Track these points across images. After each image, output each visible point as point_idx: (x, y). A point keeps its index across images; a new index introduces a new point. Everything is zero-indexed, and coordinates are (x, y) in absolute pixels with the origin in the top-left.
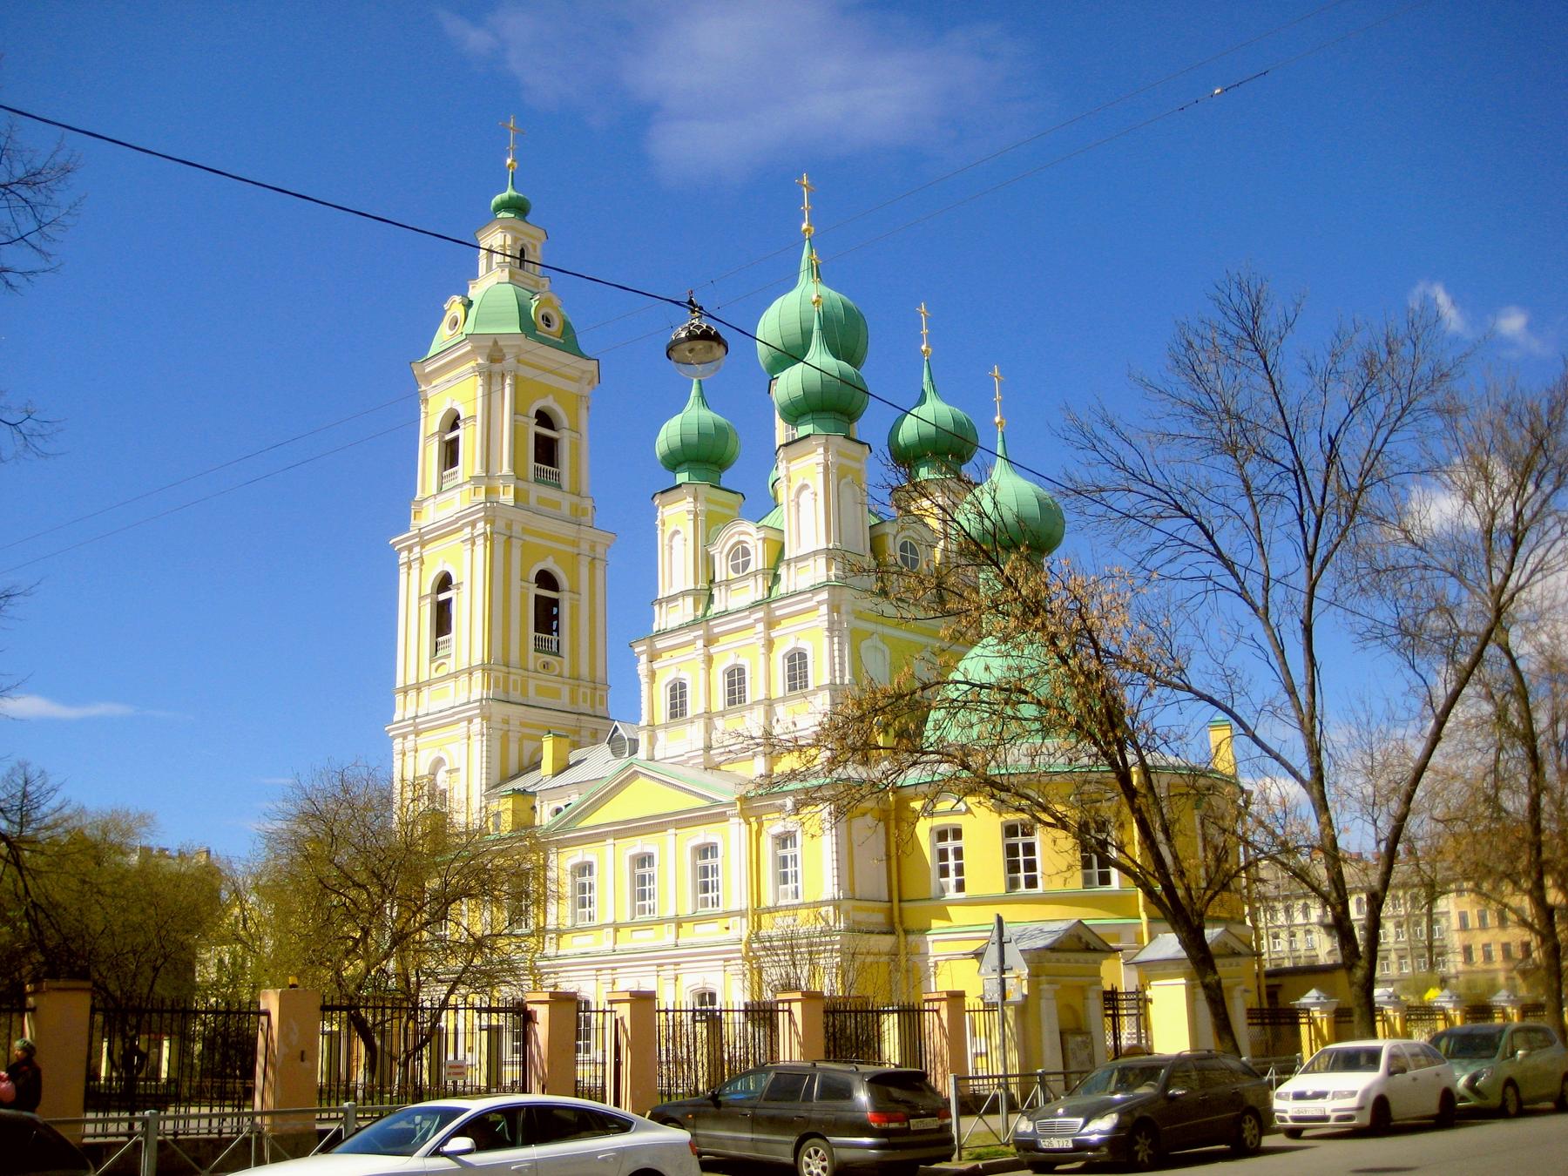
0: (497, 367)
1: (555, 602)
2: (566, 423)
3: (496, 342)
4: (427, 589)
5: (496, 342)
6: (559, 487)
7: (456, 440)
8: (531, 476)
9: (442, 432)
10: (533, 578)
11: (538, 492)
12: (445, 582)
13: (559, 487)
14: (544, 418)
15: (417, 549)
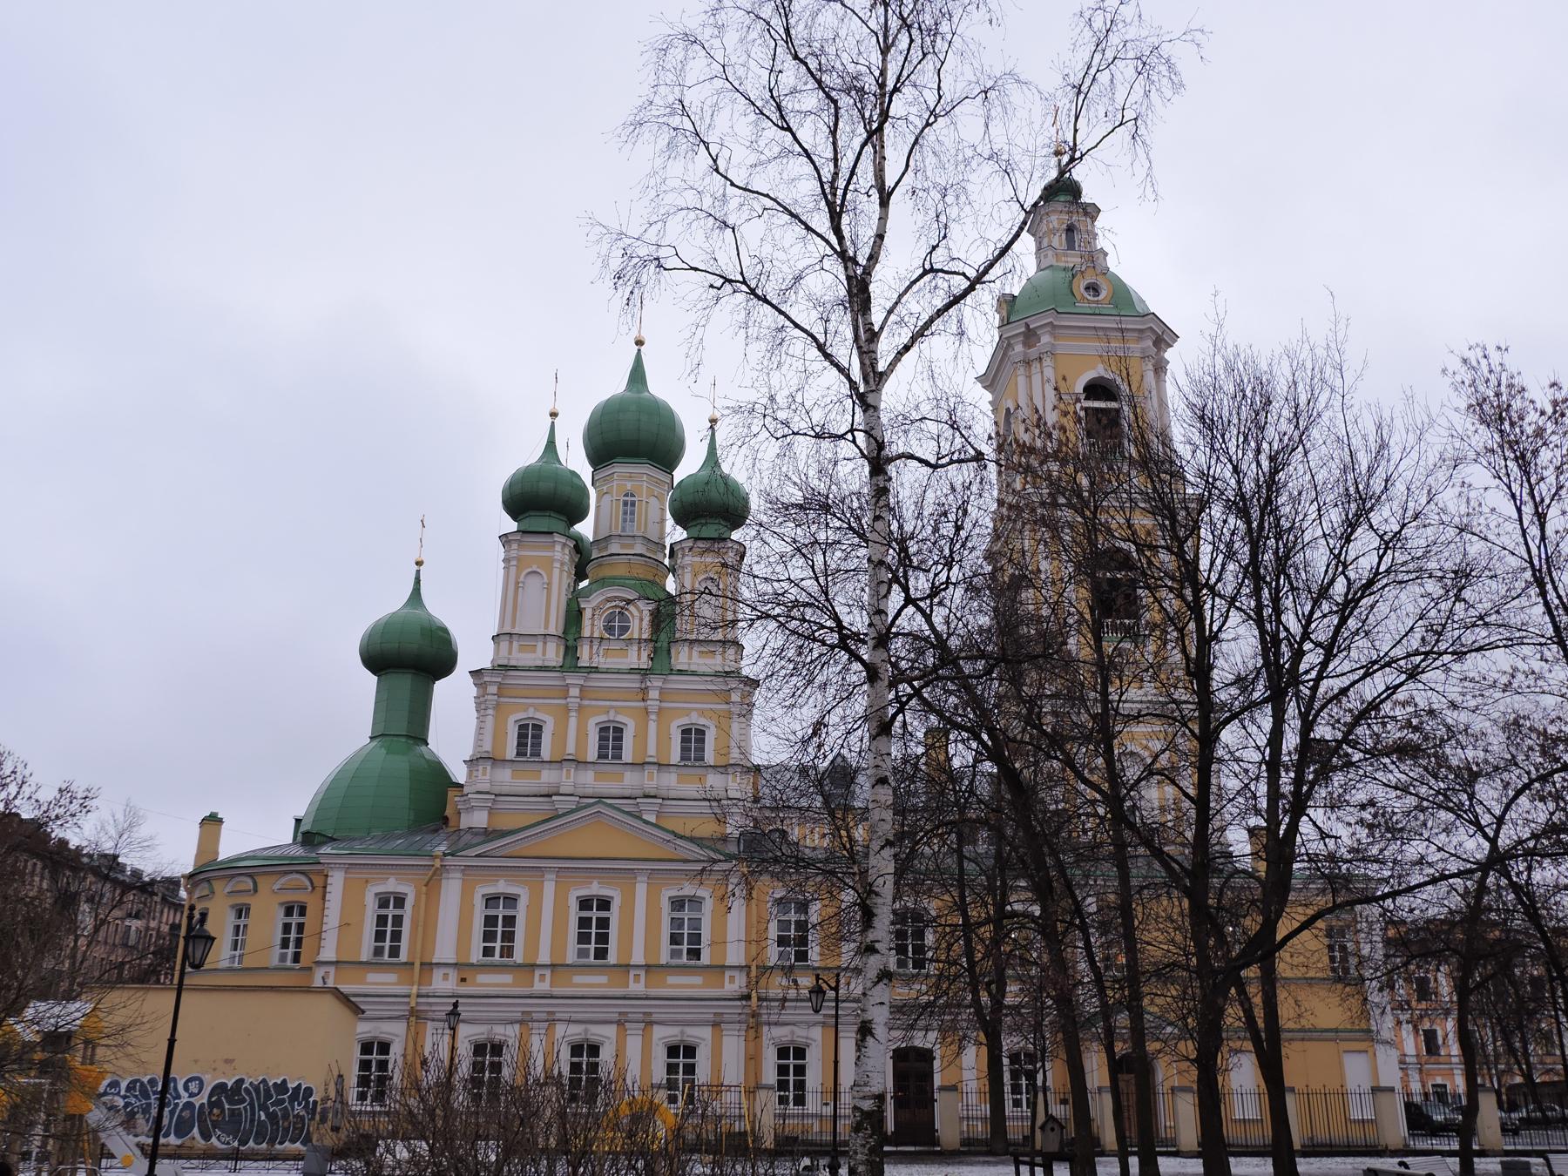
0: (1033, 352)
3: (1027, 326)
5: (1027, 326)
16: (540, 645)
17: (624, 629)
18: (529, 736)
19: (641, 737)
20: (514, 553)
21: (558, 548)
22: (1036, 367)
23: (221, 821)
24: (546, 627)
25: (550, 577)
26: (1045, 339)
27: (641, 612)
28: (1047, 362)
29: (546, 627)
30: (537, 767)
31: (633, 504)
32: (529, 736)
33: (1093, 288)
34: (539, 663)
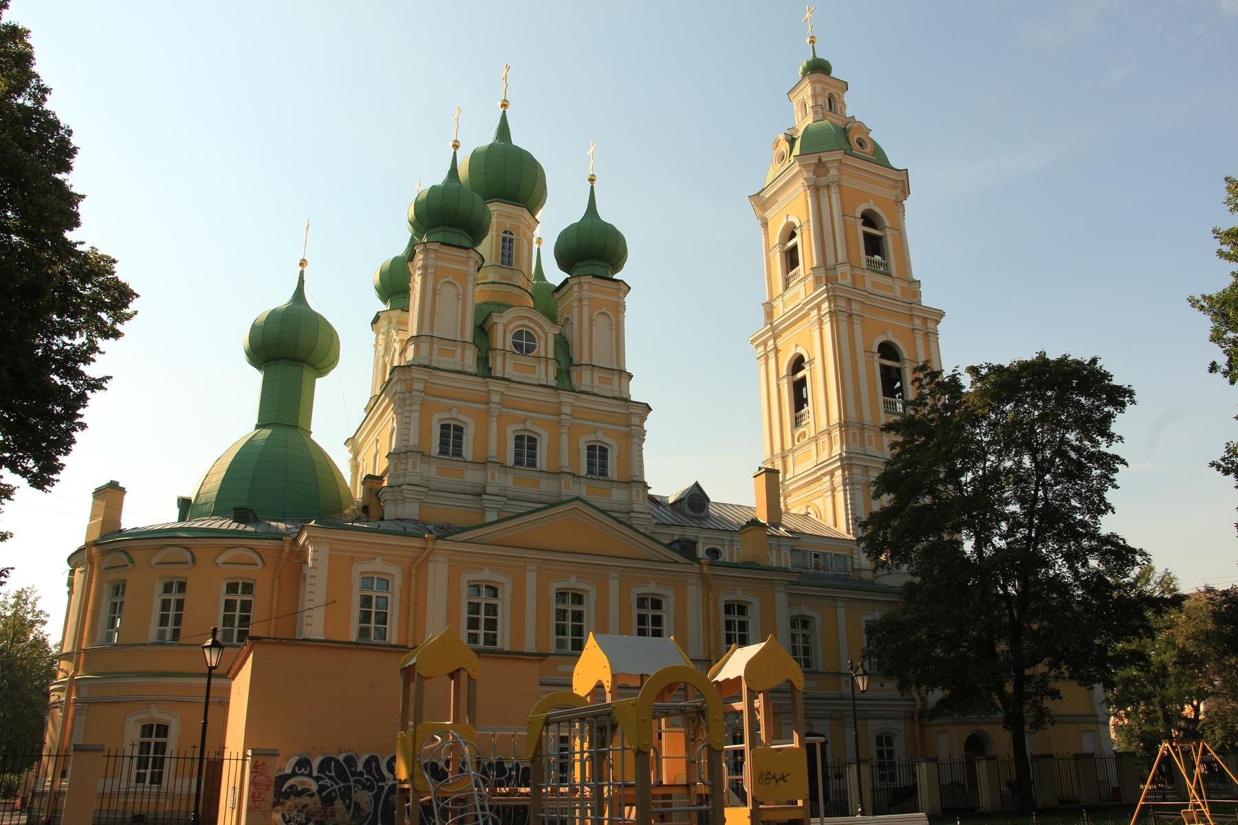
0: (823, 181)
1: (898, 370)
2: (887, 223)
3: (820, 159)
4: (784, 371)
5: (820, 159)
6: (889, 275)
7: (794, 249)
8: (864, 265)
9: (783, 243)
10: (875, 349)
11: (870, 279)
12: (798, 363)
13: (889, 275)
14: (869, 219)
15: (771, 343)
16: (459, 351)
17: (530, 349)
18: (451, 437)
19: (555, 448)
20: (431, 262)
21: (472, 263)
22: (823, 193)
23: (123, 490)
24: (462, 335)
25: (465, 290)
26: (833, 172)
27: (546, 334)
28: (834, 190)
29: (462, 335)
30: (463, 464)
31: (511, 241)
32: (451, 437)
33: (861, 143)
34: (459, 368)
